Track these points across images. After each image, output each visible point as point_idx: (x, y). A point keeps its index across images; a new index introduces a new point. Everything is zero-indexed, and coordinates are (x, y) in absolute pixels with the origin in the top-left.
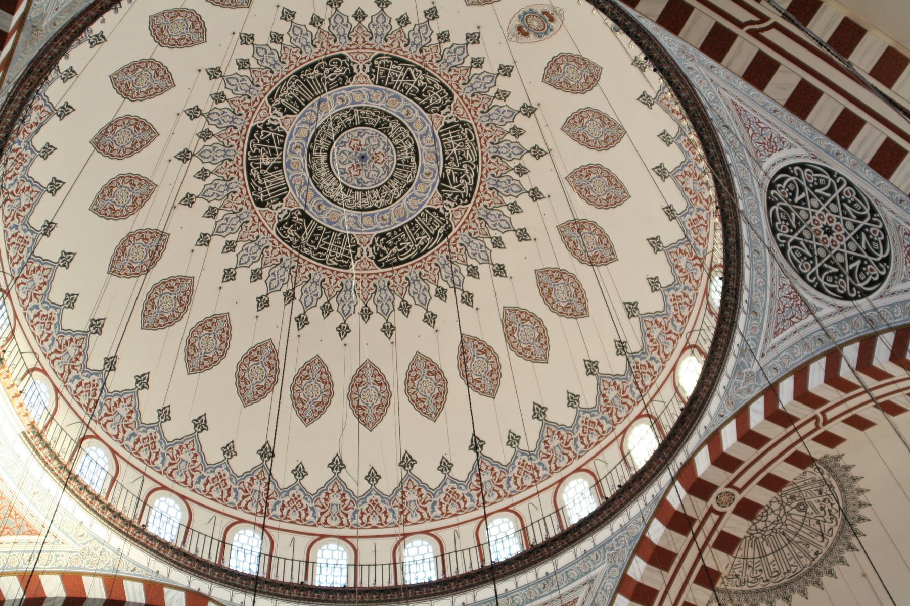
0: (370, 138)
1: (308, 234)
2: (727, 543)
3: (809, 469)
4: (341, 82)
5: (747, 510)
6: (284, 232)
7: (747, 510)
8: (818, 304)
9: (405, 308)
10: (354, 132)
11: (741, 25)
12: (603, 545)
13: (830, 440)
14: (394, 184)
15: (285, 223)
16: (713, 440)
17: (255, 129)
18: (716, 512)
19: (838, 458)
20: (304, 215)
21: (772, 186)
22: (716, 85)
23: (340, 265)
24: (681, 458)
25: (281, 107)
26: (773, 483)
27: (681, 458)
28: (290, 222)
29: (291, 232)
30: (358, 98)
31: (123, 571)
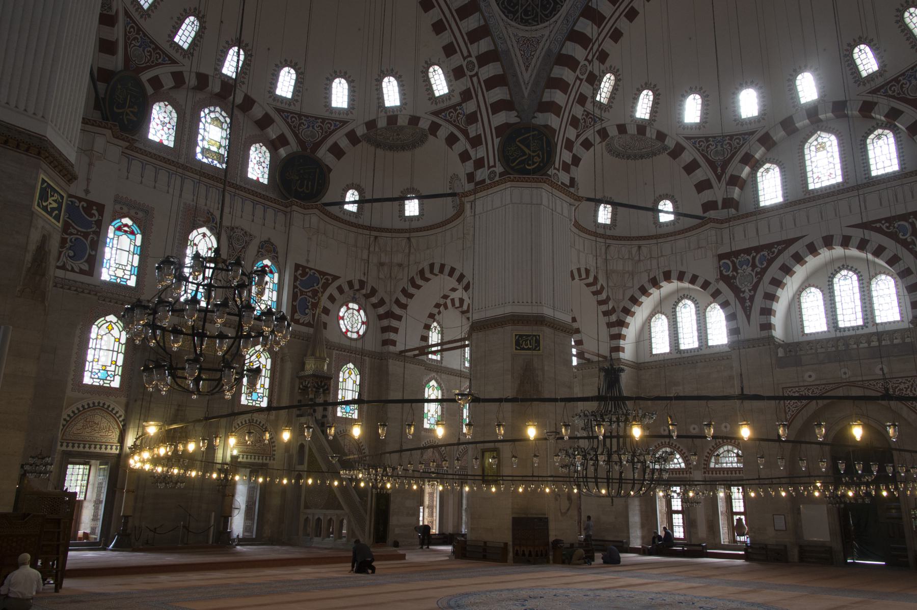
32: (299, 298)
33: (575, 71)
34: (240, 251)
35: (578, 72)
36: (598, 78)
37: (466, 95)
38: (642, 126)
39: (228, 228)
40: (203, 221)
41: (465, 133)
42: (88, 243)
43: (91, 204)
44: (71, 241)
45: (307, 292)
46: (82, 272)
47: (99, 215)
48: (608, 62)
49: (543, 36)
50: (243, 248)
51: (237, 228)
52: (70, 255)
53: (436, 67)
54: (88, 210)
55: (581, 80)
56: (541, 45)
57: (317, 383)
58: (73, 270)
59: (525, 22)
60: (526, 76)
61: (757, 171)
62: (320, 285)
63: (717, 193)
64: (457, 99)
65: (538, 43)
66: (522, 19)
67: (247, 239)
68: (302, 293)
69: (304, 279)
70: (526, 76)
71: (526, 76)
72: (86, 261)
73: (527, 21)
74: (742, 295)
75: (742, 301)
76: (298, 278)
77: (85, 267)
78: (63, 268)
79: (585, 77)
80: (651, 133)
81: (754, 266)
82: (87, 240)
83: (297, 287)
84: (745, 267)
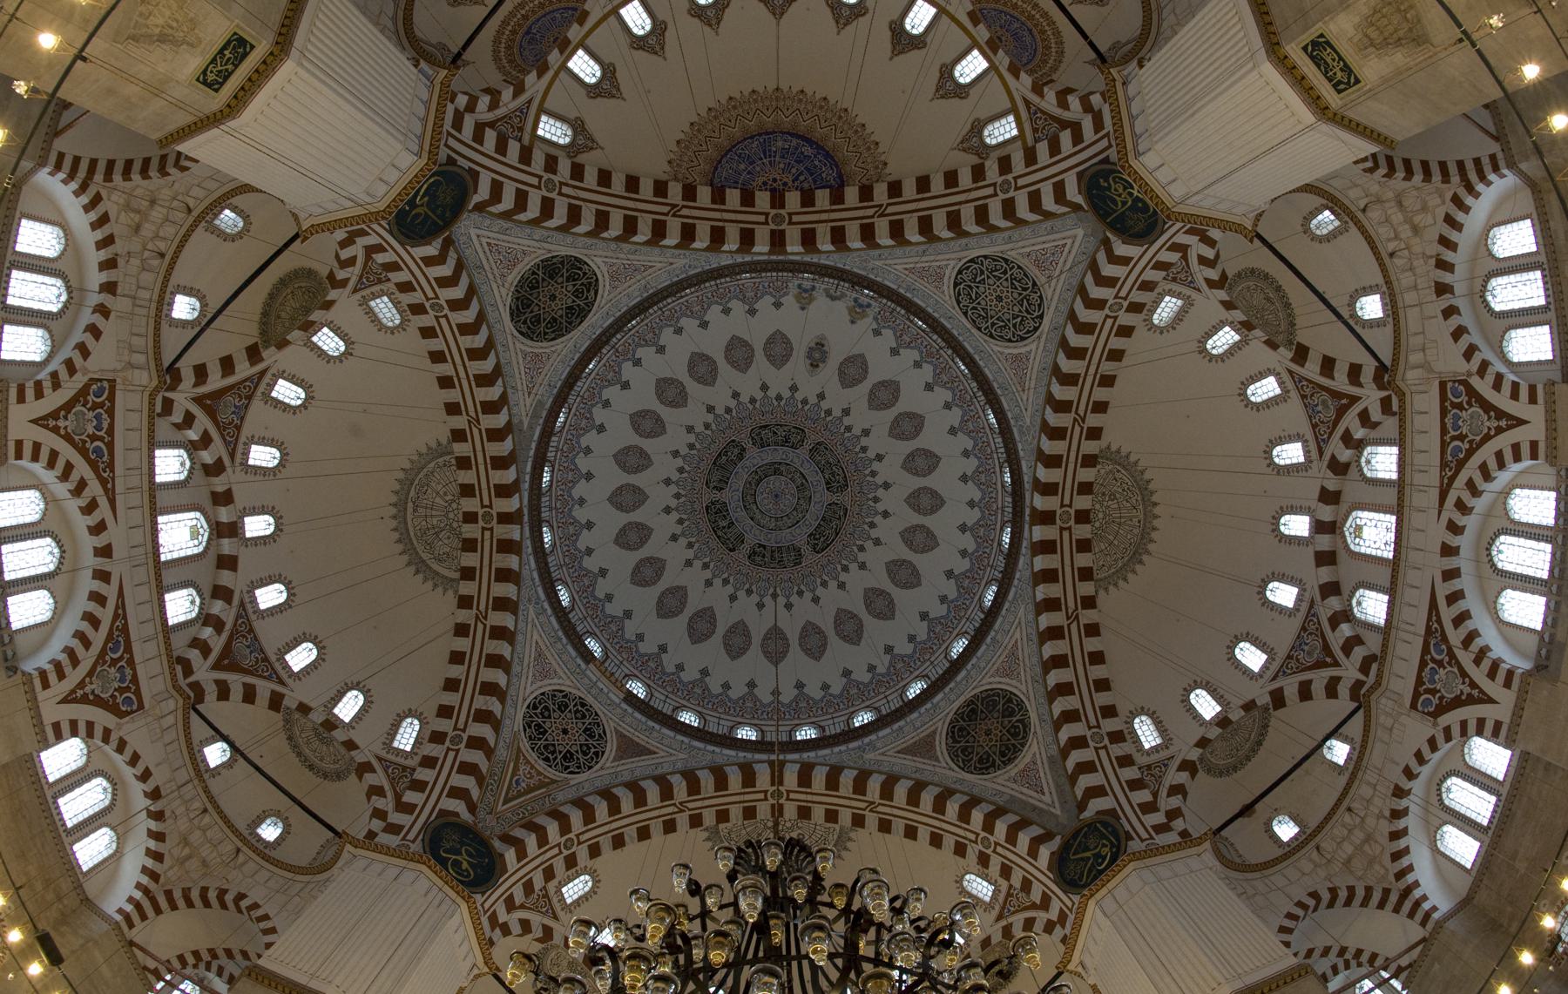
0: (774, 482)
1: (768, 555)
2: (1084, 546)
3: (1098, 467)
4: (741, 457)
5: (1083, 517)
6: (754, 560)
7: (1083, 517)
8: (1028, 349)
9: (845, 569)
10: (763, 484)
11: (873, 217)
12: (1014, 598)
13: (1095, 433)
14: (801, 502)
15: (752, 555)
16: (1036, 481)
17: (707, 508)
18: (1065, 529)
19: (1108, 447)
20: (760, 545)
21: (958, 303)
22: (890, 265)
23: (796, 564)
24: (1027, 511)
25: (715, 487)
26: (1085, 488)
27: (1027, 511)
28: (755, 553)
29: (758, 559)
30: (755, 461)
31: (720, 760)
33: (1088, 746)
35: (1091, 744)
36: (1126, 732)
37: (1006, 872)
38: (1222, 721)
41: (1034, 906)
48: (1123, 709)
49: (1034, 754)
53: (967, 877)
55: (1105, 747)
56: (1039, 762)
59: (1010, 761)
60: (1048, 799)
61: (1355, 617)
63: (1349, 671)
64: (1004, 884)
65: (1035, 763)
66: (1003, 762)
70: (1048, 799)
71: (1047, 798)
73: (1009, 760)
74: (1463, 697)
75: (1471, 700)
79: (1106, 741)
80: (1236, 715)
81: (1440, 664)
84: (1437, 677)
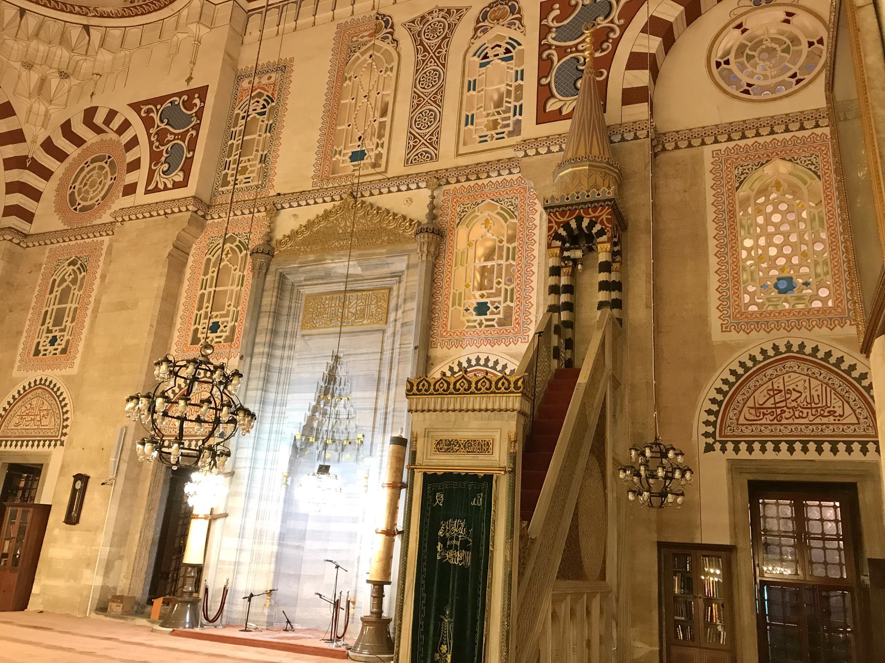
32: (556, 65)
34: (439, 47)
39: (413, 22)
40: (370, 36)
42: (185, 145)
43: (190, 93)
44: (167, 152)
45: (576, 45)
46: (176, 185)
47: (201, 102)
50: (445, 37)
51: (430, 13)
52: (165, 169)
54: (189, 105)
57: (567, 226)
58: (166, 188)
62: (615, 14)
67: (451, 20)
68: (562, 52)
69: (566, 22)
72: (181, 170)
76: (551, 28)
77: (179, 177)
78: (156, 190)
82: (184, 142)
83: (550, 46)
